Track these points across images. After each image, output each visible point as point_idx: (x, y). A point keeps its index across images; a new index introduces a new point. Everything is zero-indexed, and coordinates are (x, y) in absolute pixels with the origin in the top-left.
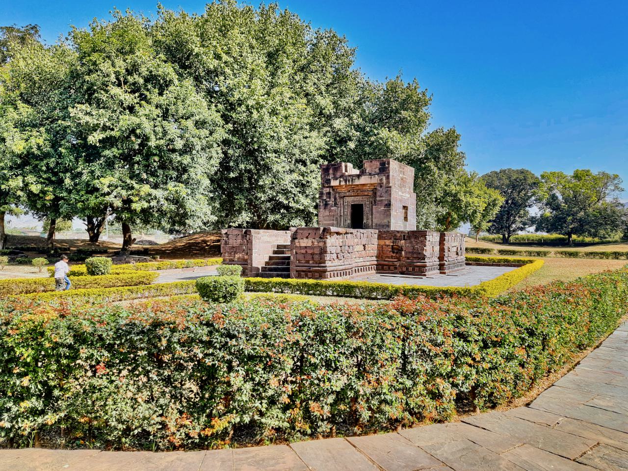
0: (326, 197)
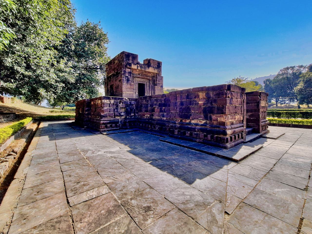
0: (128, 74)
